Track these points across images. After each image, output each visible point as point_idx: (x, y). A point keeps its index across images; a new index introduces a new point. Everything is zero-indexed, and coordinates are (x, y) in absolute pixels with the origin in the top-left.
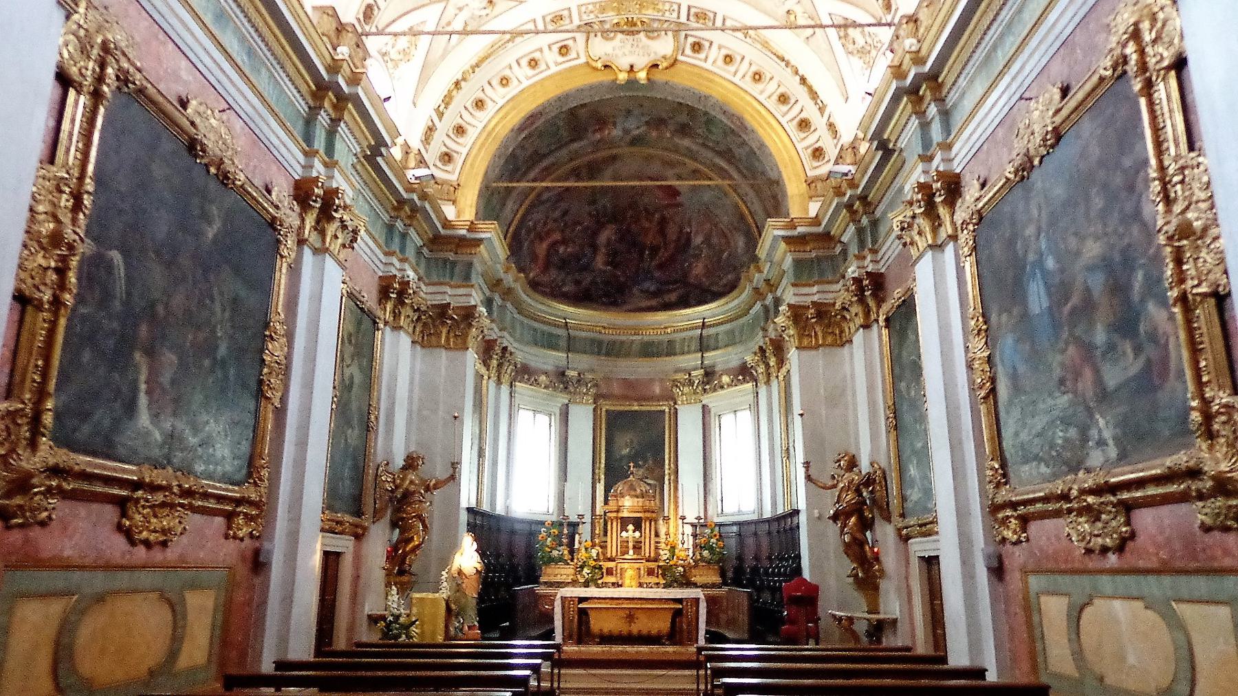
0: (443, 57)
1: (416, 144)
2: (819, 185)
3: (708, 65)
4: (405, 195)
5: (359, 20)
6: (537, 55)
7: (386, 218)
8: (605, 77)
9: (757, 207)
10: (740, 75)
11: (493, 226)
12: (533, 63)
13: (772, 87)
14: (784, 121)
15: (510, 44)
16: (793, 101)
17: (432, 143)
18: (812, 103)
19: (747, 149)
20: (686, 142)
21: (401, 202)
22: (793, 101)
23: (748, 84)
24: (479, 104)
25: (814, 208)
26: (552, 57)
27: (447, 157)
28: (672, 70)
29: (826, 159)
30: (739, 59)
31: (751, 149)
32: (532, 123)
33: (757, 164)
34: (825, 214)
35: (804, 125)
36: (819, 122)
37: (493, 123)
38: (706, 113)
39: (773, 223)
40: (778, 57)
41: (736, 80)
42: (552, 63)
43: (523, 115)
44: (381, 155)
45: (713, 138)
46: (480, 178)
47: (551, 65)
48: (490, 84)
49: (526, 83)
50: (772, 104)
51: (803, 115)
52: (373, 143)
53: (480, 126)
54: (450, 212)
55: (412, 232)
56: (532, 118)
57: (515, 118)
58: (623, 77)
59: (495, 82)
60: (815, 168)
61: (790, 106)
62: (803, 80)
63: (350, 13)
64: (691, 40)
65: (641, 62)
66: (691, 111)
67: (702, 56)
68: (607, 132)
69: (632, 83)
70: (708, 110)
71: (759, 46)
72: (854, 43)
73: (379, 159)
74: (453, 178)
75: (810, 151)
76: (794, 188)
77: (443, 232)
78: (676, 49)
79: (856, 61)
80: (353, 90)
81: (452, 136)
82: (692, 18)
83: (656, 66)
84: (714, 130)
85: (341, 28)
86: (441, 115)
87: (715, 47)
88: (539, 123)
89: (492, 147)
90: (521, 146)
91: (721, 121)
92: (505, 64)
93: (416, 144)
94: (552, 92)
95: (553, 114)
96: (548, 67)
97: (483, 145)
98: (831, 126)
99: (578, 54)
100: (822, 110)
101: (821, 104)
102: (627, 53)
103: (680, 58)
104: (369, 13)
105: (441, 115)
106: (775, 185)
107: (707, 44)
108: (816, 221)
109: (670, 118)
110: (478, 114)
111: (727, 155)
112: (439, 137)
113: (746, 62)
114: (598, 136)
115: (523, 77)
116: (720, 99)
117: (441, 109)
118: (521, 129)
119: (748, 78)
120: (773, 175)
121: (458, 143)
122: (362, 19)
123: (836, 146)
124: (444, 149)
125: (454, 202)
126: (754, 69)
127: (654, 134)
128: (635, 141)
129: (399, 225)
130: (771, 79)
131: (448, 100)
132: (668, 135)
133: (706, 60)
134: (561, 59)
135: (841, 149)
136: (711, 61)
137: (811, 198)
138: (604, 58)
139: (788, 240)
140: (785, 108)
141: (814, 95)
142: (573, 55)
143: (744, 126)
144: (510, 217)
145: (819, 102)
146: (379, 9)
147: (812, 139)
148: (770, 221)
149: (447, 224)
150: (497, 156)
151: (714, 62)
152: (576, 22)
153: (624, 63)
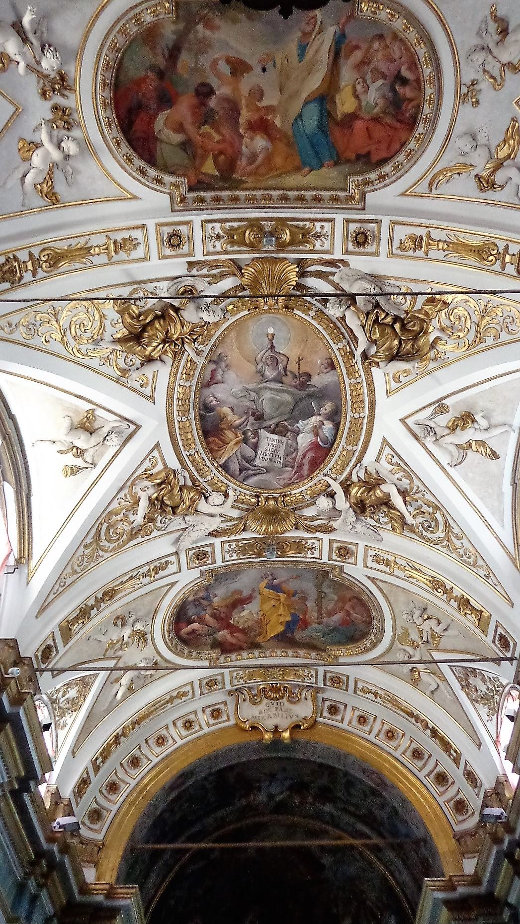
0: (108, 711)
1: (67, 792)
2: (469, 841)
3: (344, 726)
4: (45, 846)
5: (36, 656)
6: (192, 717)
7: (19, 874)
8: (253, 738)
9: (406, 877)
10: (374, 732)
11: (133, 891)
12: (188, 725)
13: (405, 743)
14: (421, 775)
15: (169, 705)
16: (426, 756)
17: (84, 796)
18: (445, 755)
19: (388, 809)
20: (328, 808)
21: (40, 854)
22: (426, 756)
23: (382, 742)
24: (135, 762)
25: (469, 866)
26: (204, 718)
27: (96, 815)
28: (312, 730)
29: (470, 812)
30: (372, 719)
31: (394, 807)
32: (183, 783)
33: (400, 825)
34: (485, 868)
35: (441, 779)
36: (456, 774)
37: (145, 781)
38: (346, 774)
39: (432, 883)
40: (408, 714)
41: (371, 737)
42: (205, 724)
43: (174, 772)
44: (29, 790)
45: (355, 801)
46: (126, 838)
47: (204, 726)
48: (147, 742)
49: (180, 742)
50: (407, 760)
51: (438, 769)
52: (23, 774)
53: (133, 783)
54: (90, 874)
55: (44, 894)
56: (184, 776)
57: (167, 776)
58: (268, 736)
59: (151, 741)
60: (463, 821)
61: (425, 760)
62: (434, 733)
63: (28, 650)
64: (327, 704)
65: (284, 723)
66: (331, 770)
67: (339, 718)
68: (252, 798)
69: (277, 743)
70: (347, 769)
71: (389, 705)
72: (476, 690)
73: (26, 797)
74: (100, 837)
75: (452, 803)
76: (443, 845)
77: (78, 897)
78: (315, 712)
79: (483, 711)
80: (14, 710)
81: (105, 792)
82: (328, 683)
83: (298, 726)
84: (353, 791)
85: (19, 661)
86: (97, 769)
87: (349, 709)
88: (191, 782)
89: (143, 804)
90: (171, 808)
91: (361, 781)
92: (164, 723)
93: (67, 792)
94: (204, 751)
95: (203, 775)
96: (201, 728)
97: (133, 803)
98: (470, 776)
99: (228, 717)
100: (457, 761)
101: (455, 755)
102: (272, 715)
103: (319, 719)
104: (47, 652)
105: (97, 769)
106: (425, 841)
107: (342, 707)
108: (475, 880)
109: (312, 782)
110: (133, 772)
111: (370, 820)
112: (91, 791)
113: (379, 721)
114: (244, 802)
115: (178, 737)
116: (358, 755)
117: (98, 762)
118: (172, 787)
119: (381, 736)
120: (419, 833)
121: (109, 800)
122: (40, 657)
123: (478, 795)
124: (95, 806)
125: (96, 864)
126: (386, 727)
127: (297, 799)
128: (281, 808)
129: (32, 884)
130: (403, 735)
131: (105, 753)
132: (310, 800)
133: (342, 721)
134: (212, 721)
135: (485, 796)
136: (347, 721)
137: (463, 854)
138: (251, 720)
139: (448, 903)
140: (420, 764)
141: (446, 746)
142: (225, 718)
143: (384, 784)
144: (152, 892)
145: (452, 752)
146: (57, 652)
147: (452, 792)
148: (428, 881)
149: (84, 888)
150: (145, 815)
151: (350, 722)
152: (228, 687)
153: (270, 724)
